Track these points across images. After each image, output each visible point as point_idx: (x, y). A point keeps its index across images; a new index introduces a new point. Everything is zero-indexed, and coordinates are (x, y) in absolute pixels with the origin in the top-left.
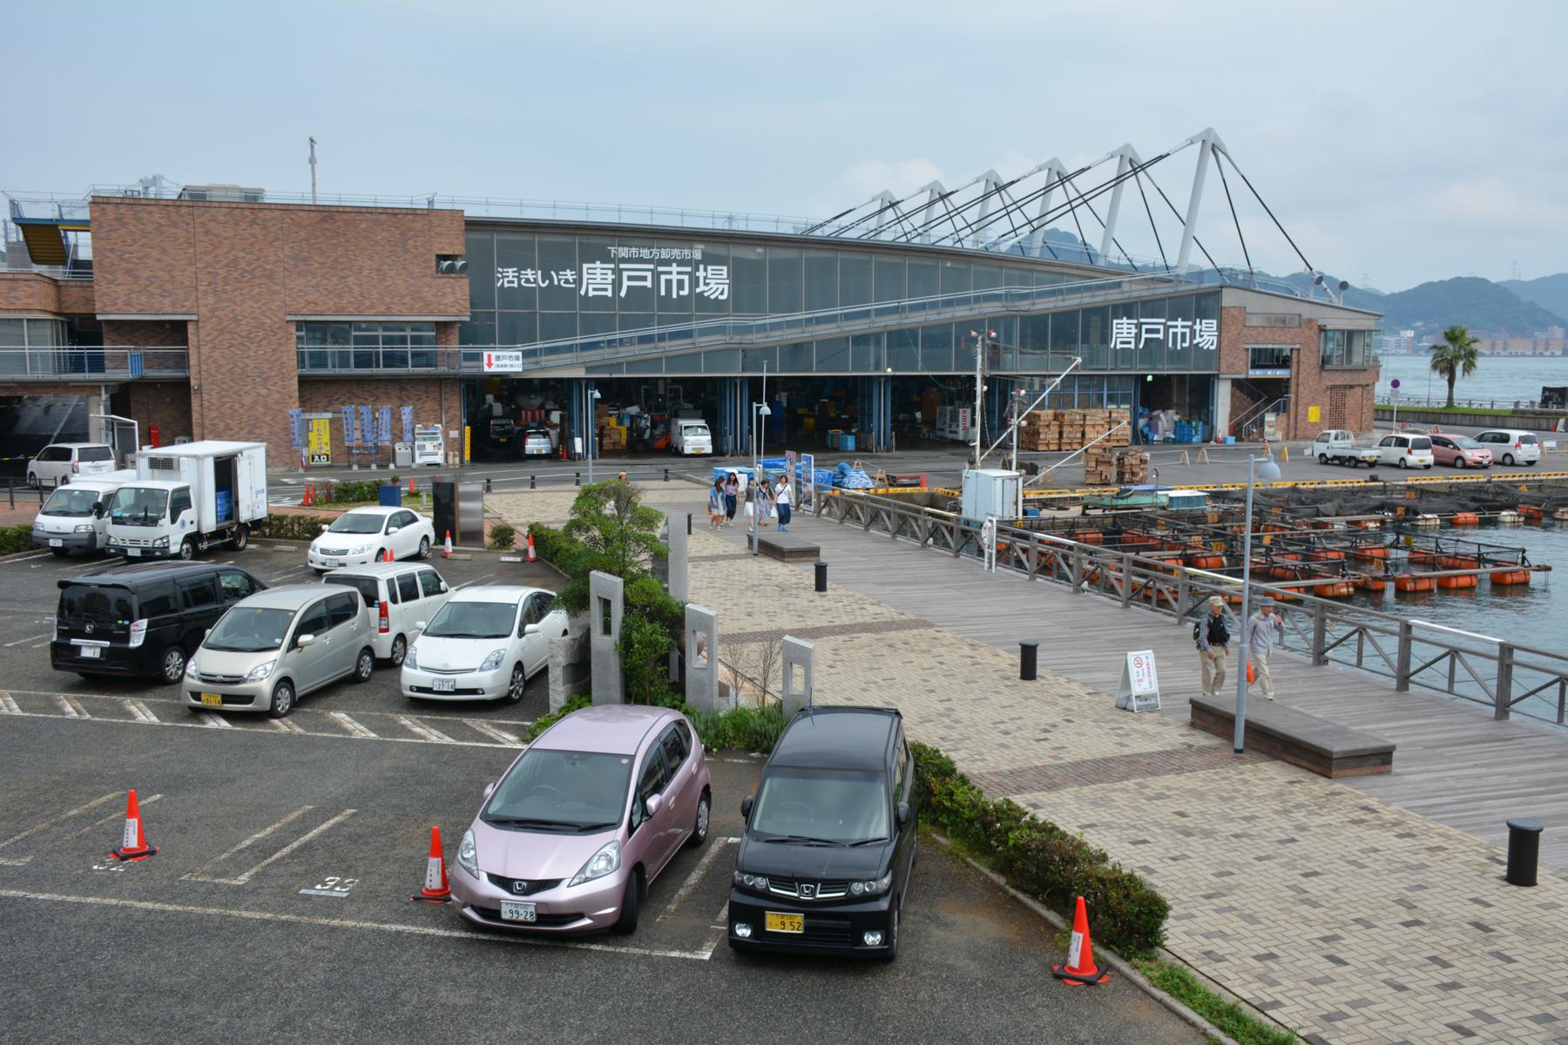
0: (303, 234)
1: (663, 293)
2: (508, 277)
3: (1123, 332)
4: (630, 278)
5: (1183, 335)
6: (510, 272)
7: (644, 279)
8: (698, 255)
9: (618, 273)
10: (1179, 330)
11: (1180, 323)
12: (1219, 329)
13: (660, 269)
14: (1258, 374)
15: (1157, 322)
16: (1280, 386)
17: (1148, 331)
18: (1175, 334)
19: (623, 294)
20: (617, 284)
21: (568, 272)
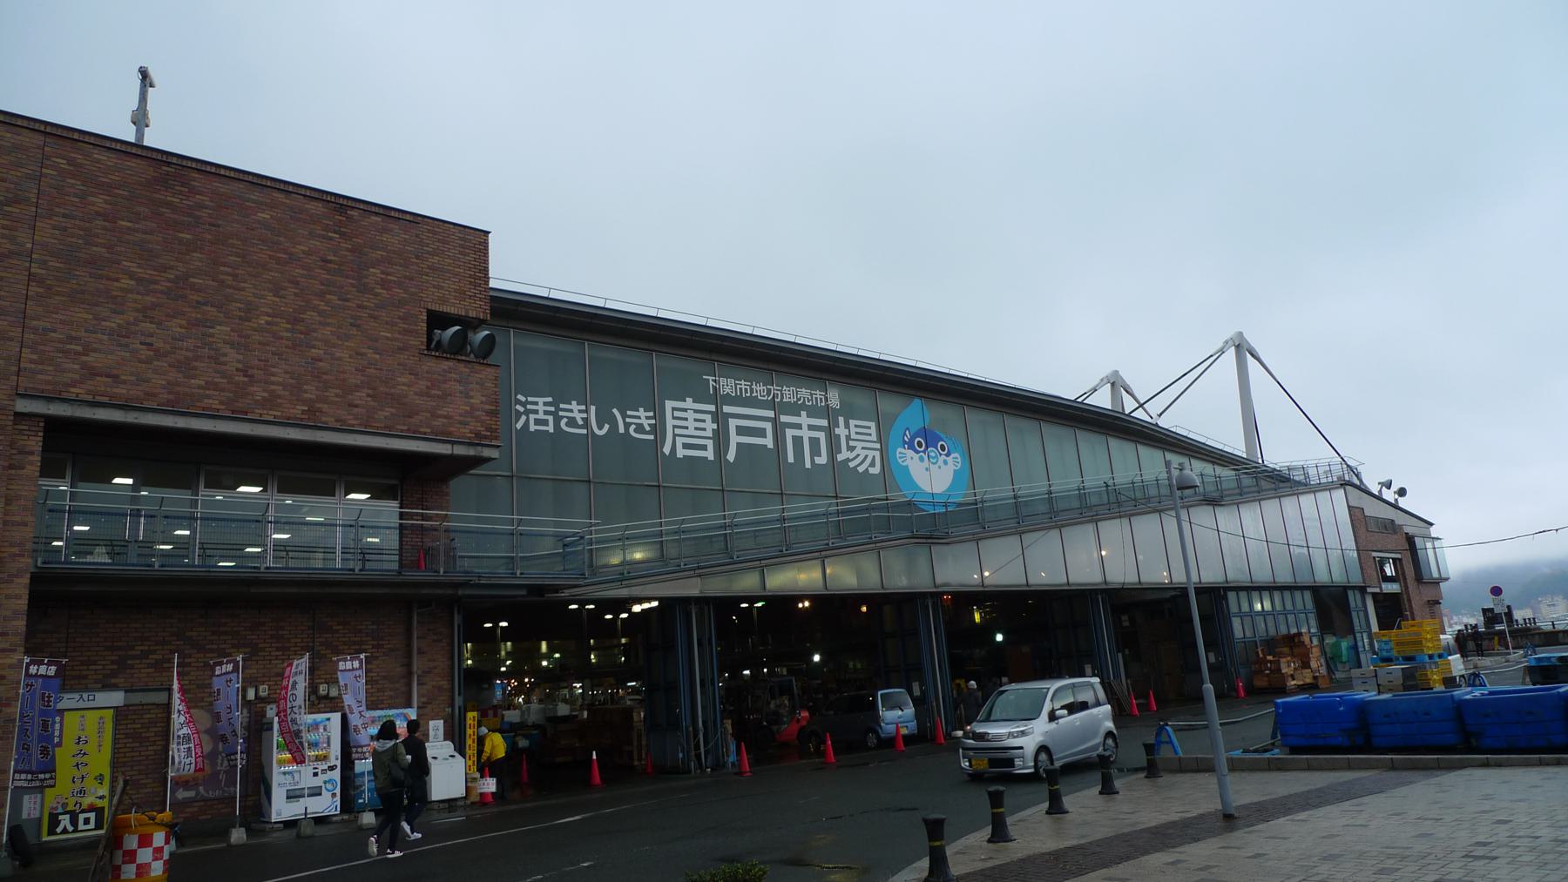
0: (99, 202)
1: (791, 459)
2: (537, 413)
4: (741, 431)
6: (541, 404)
9: (720, 418)
13: (784, 419)
19: (731, 456)
20: (720, 439)
21: (641, 412)
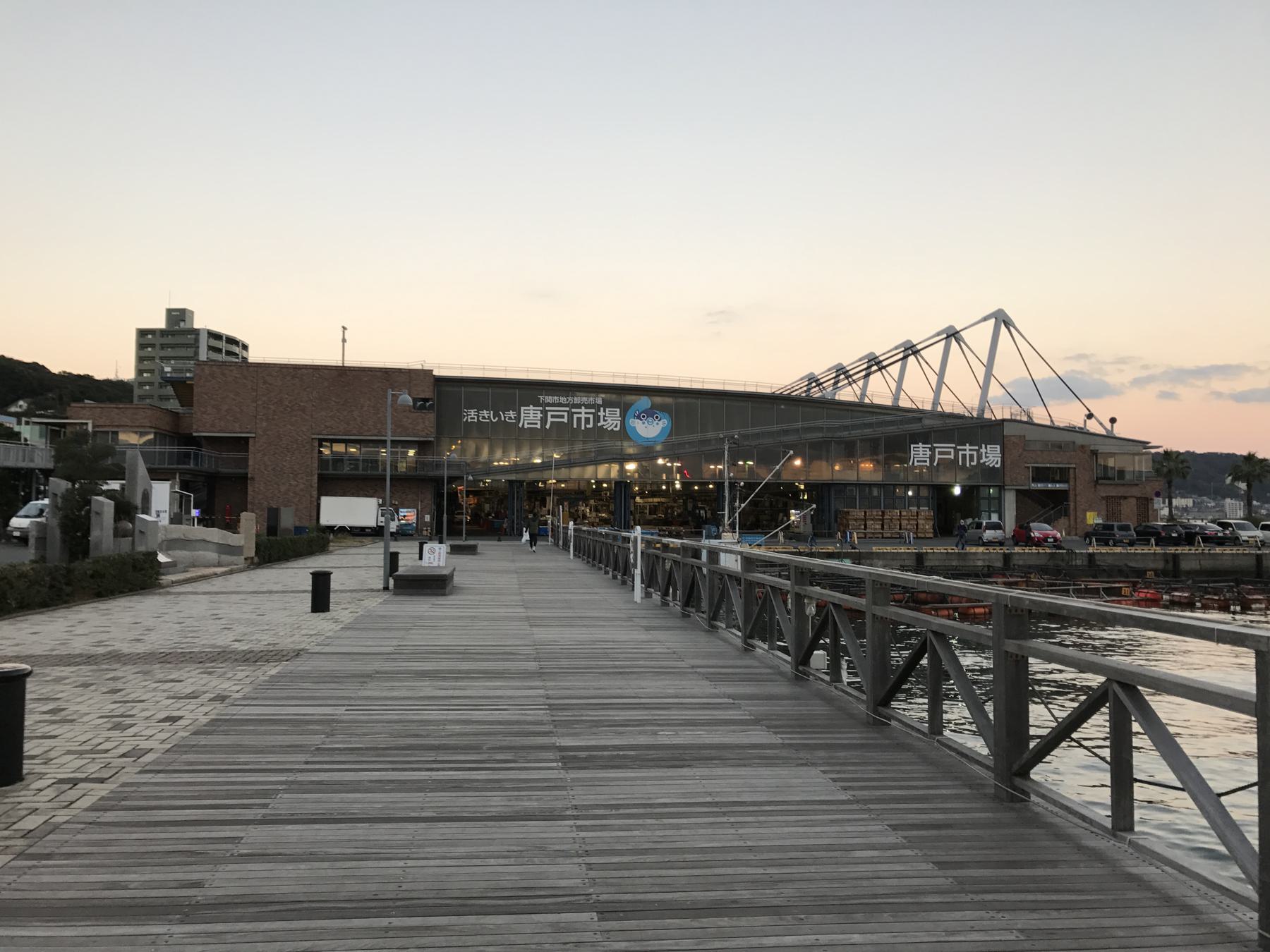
3: (920, 453)
4: (553, 416)
5: (971, 457)
6: (473, 412)
7: (563, 417)
8: (599, 402)
9: (545, 413)
10: (968, 453)
11: (967, 447)
12: (1003, 452)
14: (1040, 486)
15: (948, 448)
16: (1063, 495)
17: (940, 453)
18: (964, 456)
19: (548, 426)
20: (544, 420)
